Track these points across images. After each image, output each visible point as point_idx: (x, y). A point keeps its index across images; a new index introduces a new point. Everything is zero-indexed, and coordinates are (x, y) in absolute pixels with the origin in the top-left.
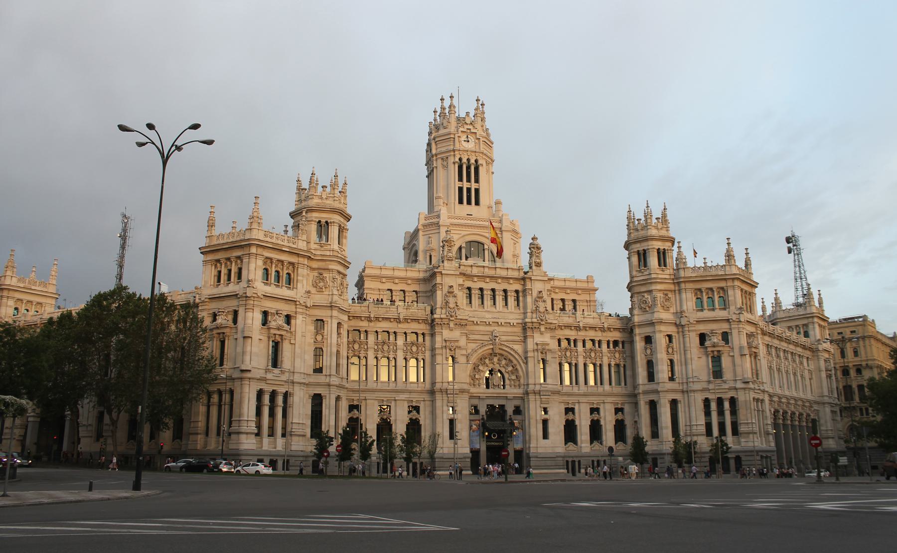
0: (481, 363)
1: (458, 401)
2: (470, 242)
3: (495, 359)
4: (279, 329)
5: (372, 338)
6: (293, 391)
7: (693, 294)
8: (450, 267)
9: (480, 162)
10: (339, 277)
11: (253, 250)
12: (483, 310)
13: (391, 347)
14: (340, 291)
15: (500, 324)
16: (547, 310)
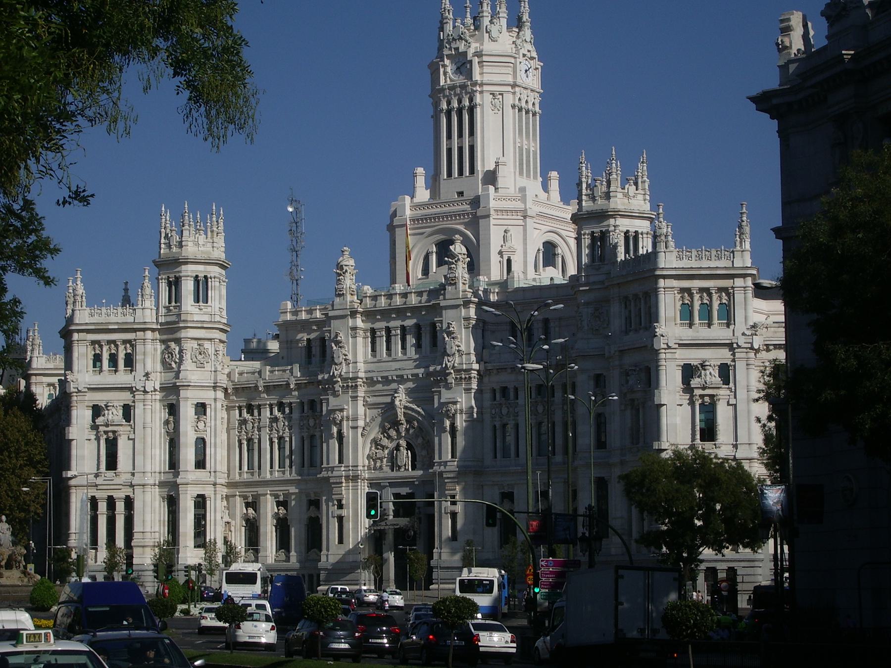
0: (384, 436)
1: (344, 492)
2: (443, 241)
3: (403, 429)
4: (107, 425)
5: (266, 413)
6: (134, 494)
7: (623, 305)
8: (341, 304)
9: (474, 101)
10: (194, 344)
11: (76, 336)
12: (390, 359)
13: (286, 423)
14: (198, 362)
15: (405, 377)
16: (459, 351)
